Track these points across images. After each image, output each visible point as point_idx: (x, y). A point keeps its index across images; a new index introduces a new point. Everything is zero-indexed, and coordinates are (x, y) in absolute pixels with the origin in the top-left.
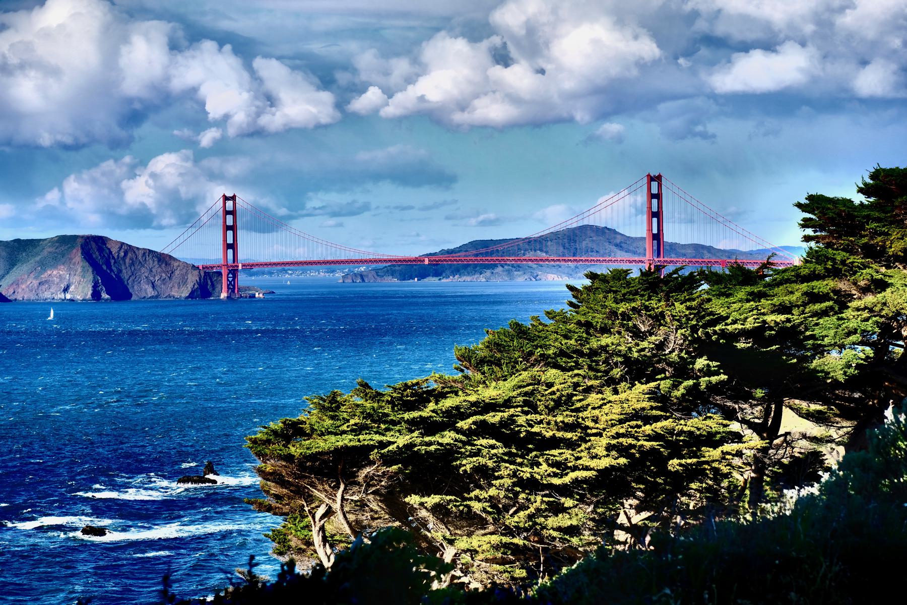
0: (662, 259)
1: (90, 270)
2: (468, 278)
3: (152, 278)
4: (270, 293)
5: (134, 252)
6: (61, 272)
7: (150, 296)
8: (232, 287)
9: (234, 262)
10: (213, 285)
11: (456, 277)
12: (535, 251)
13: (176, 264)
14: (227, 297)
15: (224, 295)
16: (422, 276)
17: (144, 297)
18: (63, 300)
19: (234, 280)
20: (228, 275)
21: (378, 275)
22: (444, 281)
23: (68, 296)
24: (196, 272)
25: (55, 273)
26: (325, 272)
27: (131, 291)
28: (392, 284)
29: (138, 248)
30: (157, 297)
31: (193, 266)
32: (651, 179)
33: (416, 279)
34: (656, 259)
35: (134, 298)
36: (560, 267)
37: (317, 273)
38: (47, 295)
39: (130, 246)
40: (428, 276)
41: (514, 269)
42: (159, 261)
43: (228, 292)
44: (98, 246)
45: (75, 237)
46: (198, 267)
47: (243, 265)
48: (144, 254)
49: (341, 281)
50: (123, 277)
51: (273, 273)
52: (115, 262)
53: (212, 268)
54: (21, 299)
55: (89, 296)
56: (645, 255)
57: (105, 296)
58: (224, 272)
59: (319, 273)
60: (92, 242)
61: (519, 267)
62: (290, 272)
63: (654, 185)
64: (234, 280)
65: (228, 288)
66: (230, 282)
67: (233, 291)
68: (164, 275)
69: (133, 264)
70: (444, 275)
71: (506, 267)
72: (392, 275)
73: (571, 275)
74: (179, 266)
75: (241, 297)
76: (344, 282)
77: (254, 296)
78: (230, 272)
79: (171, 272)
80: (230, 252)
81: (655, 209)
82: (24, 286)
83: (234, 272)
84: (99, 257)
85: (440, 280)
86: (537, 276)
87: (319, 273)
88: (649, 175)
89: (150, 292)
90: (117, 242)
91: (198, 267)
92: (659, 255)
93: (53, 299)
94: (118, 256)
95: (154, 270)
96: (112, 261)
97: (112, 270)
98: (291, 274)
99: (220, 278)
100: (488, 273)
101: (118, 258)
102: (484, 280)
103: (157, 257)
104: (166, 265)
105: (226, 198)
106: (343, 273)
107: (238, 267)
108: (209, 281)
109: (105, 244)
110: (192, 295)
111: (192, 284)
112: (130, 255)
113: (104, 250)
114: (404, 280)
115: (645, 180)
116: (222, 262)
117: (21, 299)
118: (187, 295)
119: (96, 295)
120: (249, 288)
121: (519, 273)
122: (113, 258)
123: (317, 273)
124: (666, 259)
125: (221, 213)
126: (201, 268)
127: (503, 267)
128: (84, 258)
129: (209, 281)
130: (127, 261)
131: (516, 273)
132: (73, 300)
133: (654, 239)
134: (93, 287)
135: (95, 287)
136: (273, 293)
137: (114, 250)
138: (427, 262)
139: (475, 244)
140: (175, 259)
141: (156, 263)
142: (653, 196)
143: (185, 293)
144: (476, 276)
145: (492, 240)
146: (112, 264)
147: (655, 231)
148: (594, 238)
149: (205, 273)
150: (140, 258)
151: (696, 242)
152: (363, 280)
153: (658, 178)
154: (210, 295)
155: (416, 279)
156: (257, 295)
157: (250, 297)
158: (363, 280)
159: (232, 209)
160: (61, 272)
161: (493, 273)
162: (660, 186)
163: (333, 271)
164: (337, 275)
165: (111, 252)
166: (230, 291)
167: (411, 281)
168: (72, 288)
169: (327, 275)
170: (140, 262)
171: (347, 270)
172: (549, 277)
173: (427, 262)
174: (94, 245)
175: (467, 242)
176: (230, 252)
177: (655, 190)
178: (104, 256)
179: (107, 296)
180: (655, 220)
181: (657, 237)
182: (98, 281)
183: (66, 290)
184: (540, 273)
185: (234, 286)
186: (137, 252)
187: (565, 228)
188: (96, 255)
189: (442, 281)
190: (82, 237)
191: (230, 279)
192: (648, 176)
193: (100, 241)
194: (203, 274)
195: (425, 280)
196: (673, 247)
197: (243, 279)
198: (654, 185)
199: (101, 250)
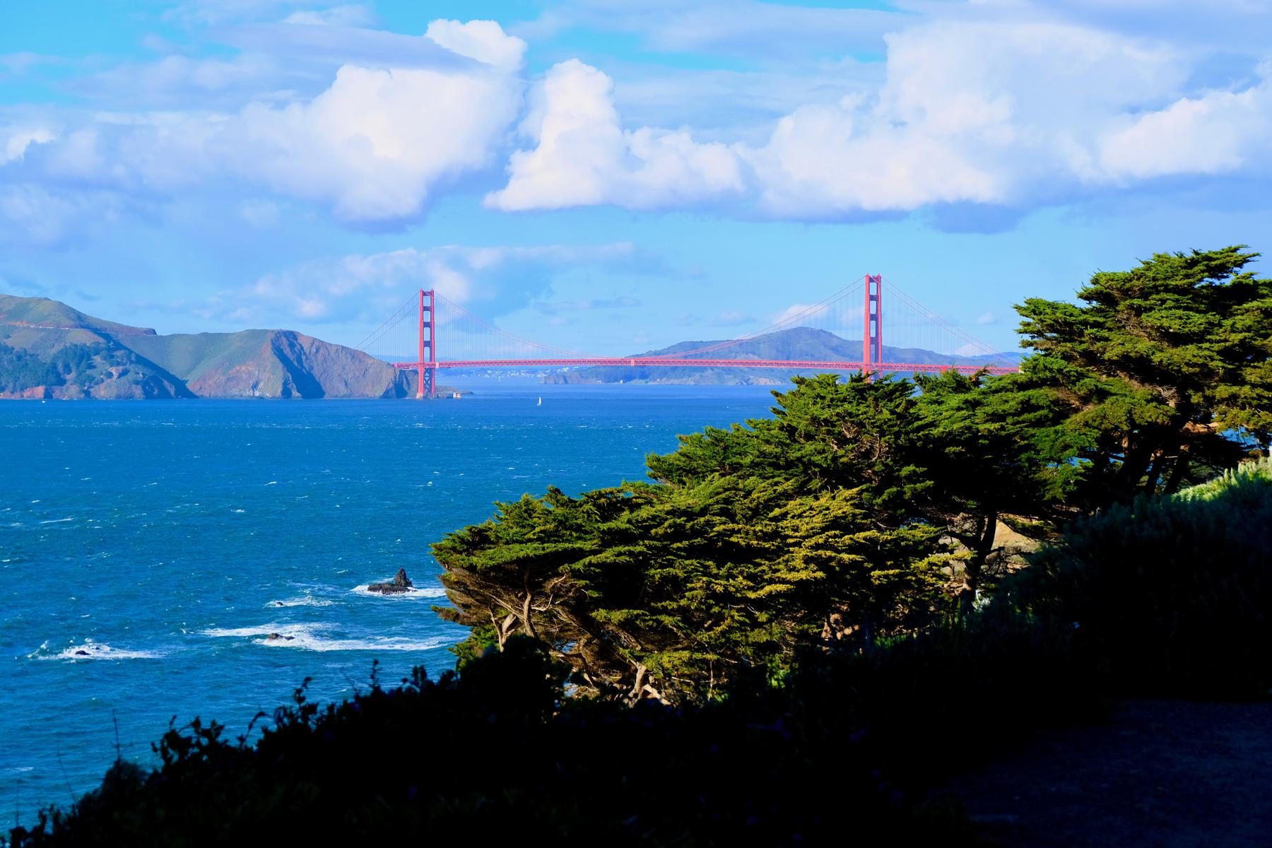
0: (880, 364)
1: (281, 365)
2: (676, 382)
3: (345, 376)
4: (468, 394)
5: (327, 348)
6: (250, 368)
7: (342, 394)
8: (429, 386)
9: (431, 360)
10: (408, 383)
11: (664, 380)
12: (747, 353)
13: (370, 362)
14: (424, 397)
15: (419, 395)
16: (628, 378)
17: (337, 396)
18: (252, 397)
19: (430, 379)
20: (425, 373)
21: (582, 377)
22: (651, 383)
23: (257, 394)
24: (391, 370)
25: (243, 368)
26: (526, 372)
27: (323, 388)
28: (596, 385)
29: (330, 344)
30: (350, 395)
31: (389, 364)
32: (871, 280)
33: (621, 381)
34: (874, 365)
35: (326, 397)
36: (773, 371)
37: (518, 374)
38: (235, 392)
39: (322, 342)
40: (634, 378)
41: (725, 373)
42: (353, 357)
43: (424, 392)
44: (288, 340)
45: (265, 332)
46: (393, 366)
47: (440, 364)
48: (337, 350)
49: (543, 382)
50: (315, 375)
51: (472, 373)
52: (307, 359)
53: (408, 366)
54: (208, 395)
55: (279, 393)
56: (862, 359)
57: (295, 394)
58: (421, 370)
59: (520, 374)
60: (283, 337)
61: (730, 370)
62: (489, 372)
63: (873, 285)
64: (430, 379)
65: (425, 388)
66: (427, 382)
67: (430, 391)
68: (357, 373)
69: (325, 360)
70: (651, 377)
71: (716, 370)
72: (597, 376)
73: (784, 379)
74: (372, 364)
75: (438, 397)
76: (546, 383)
77: (451, 397)
78: (427, 370)
79: (364, 370)
80: (427, 349)
81: (873, 311)
82: (211, 382)
83: (430, 371)
84: (290, 353)
85: (646, 382)
86: (749, 380)
87: (520, 374)
88: (867, 276)
89: (343, 390)
90: (308, 337)
91: (393, 366)
92: (876, 360)
93: (242, 396)
94: (310, 351)
95: (347, 368)
96: (304, 357)
97: (304, 367)
98: (490, 374)
99: (416, 377)
100: (697, 375)
101: (310, 354)
102: (693, 383)
103: (351, 354)
104: (360, 362)
105: (424, 294)
106: (545, 373)
107: (435, 365)
108: (404, 380)
109: (296, 340)
110: (386, 395)
111: (387, 383)
112: (322, 351)
113: (295, 345)
114: (608, 382)
115: (864, 281)
116: (418, 360)
117: (208, 395)
118: (382, 394)
119: (286, 393)
120: (446, 388)
121: (729, 376)
122: (305, 354)
123: (518, 374)
124: (884, 364)
125: (419, 310)
126: (396, 366)
127: (713, 370)
128: (275, 353)
129: (404, 380)
130: (319, 356)
131: (726, 376)
132: (262, 398)
133: (872, 343)
134: (283, 384)
135: (285, 384)
136: (472, 393)
137: (306, 347)
138: (633, 361)
139: (682, 345)
140: (369, 357)
141: (349, 360)
142: (872, 298)
143: (379, 392)
144: (684, 379)
145: (701, 342)
146: (304, 360)
147: (873, 334)
148: (809, 341)
149: (401, 371)
150: (332, 353)
151: (916, 347)
152: (566, 382)
153: (876, 280)
154: (405, 394)
155: (621, 381)
156: (454, 396)
157: (448, 398)
158: (566, 382)
159: (429, 305)
160: (250, 368)
161: (702, 376)
162: (879, 287)
163: (534, 372)
164: (538, 376)
165: (302, 348)
166: (427, 390)
167: (617, 383)
168: (261, 385)
169: (528, 375)
170: (333, 359)
171: (549, 371)
172: (761, 382)
173: (633, 364)
174: (284, 340)
175: (675, 344)
176: (427, 349)
177: (873, 292)
178: (295, 352)
179: (298, 394)
180: (873, 323)
181: (875, 341)
182: (289, 378)
183: (255, 387)
184: (751, 377)
185: (431, 385)
186: (329, 348)
187: (778, 330)
188: (287, 351)
189: (649, 384)
190: (273, 331)
191: (427, 379)
192: (867, 276)
193: (292, 337)
194: (398, 373)
195: (631, 382)
196: (891, 350)
197: (439, 381)
198: (873, 285)
199: (292, 345)
